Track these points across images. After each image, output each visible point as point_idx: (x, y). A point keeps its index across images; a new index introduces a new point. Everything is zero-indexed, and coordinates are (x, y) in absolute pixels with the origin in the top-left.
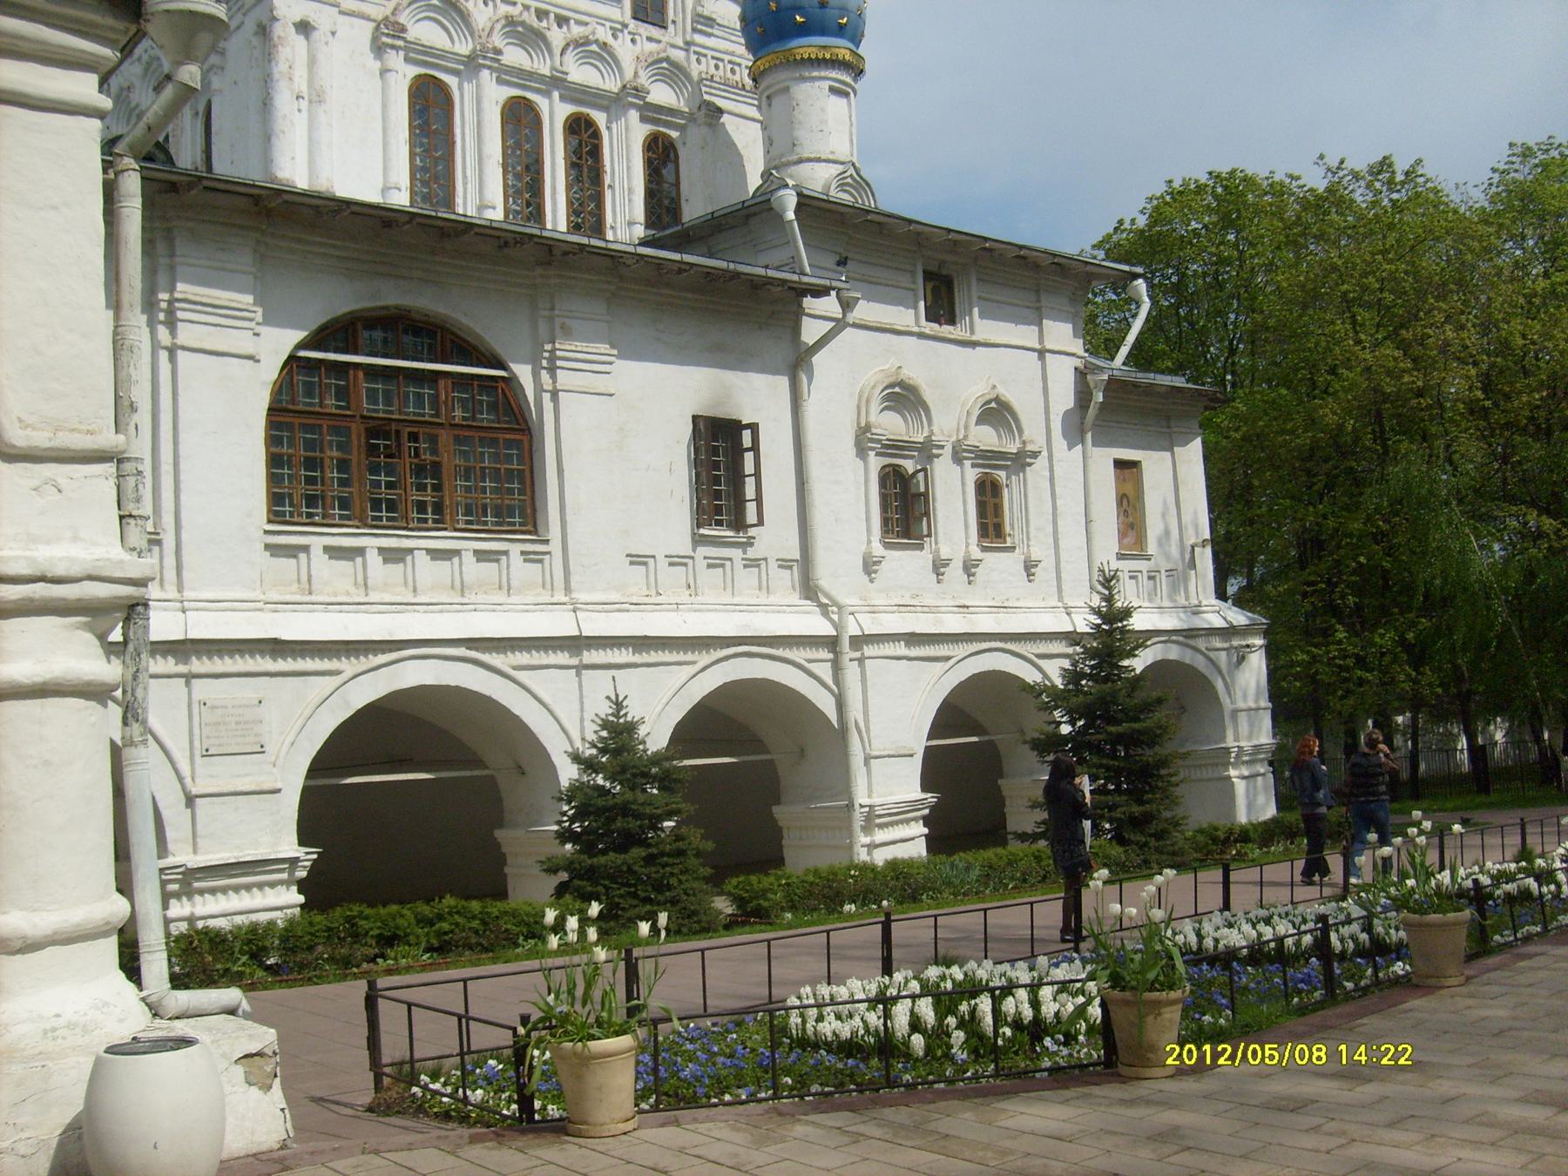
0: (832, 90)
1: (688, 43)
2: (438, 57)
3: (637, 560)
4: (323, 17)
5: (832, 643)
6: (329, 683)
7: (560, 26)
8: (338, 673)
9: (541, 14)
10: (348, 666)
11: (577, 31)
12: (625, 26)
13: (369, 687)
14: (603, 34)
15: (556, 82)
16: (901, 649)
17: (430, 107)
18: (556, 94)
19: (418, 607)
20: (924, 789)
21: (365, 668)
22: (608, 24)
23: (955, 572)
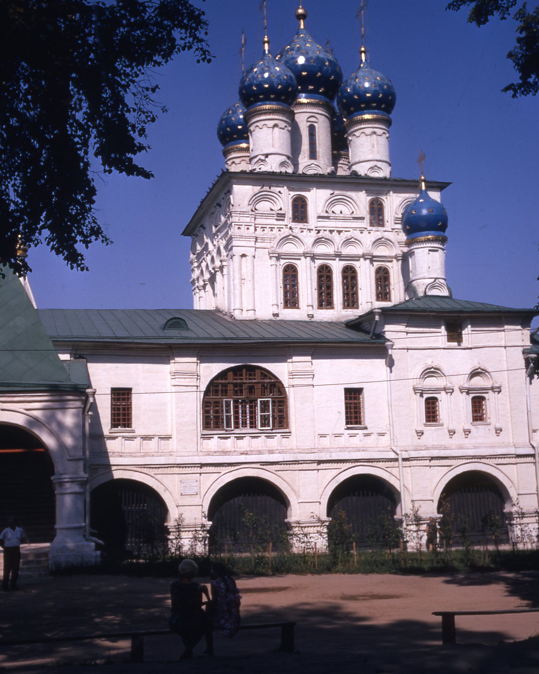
0: (430, 250)
1: (393, 229)
2: (291, 256)
3: (323, 436)
4: (250, 252)
5: (396, 460)
6: (216, 476)
7: (339, 234)
8: (220, 473)
9: (331, 232)
10: (224, 470)
11: (345, 235)
12: (366, 229)
13: (228, 476)
14: (357, 234)
15: (338, 256)
16: (427, 463)
17: (290, 274)
18: (337, 259)
19: (248, 452)
20: (439, 512)
21: (216, 471)
22: (358, 229)
23: (460, 434)
